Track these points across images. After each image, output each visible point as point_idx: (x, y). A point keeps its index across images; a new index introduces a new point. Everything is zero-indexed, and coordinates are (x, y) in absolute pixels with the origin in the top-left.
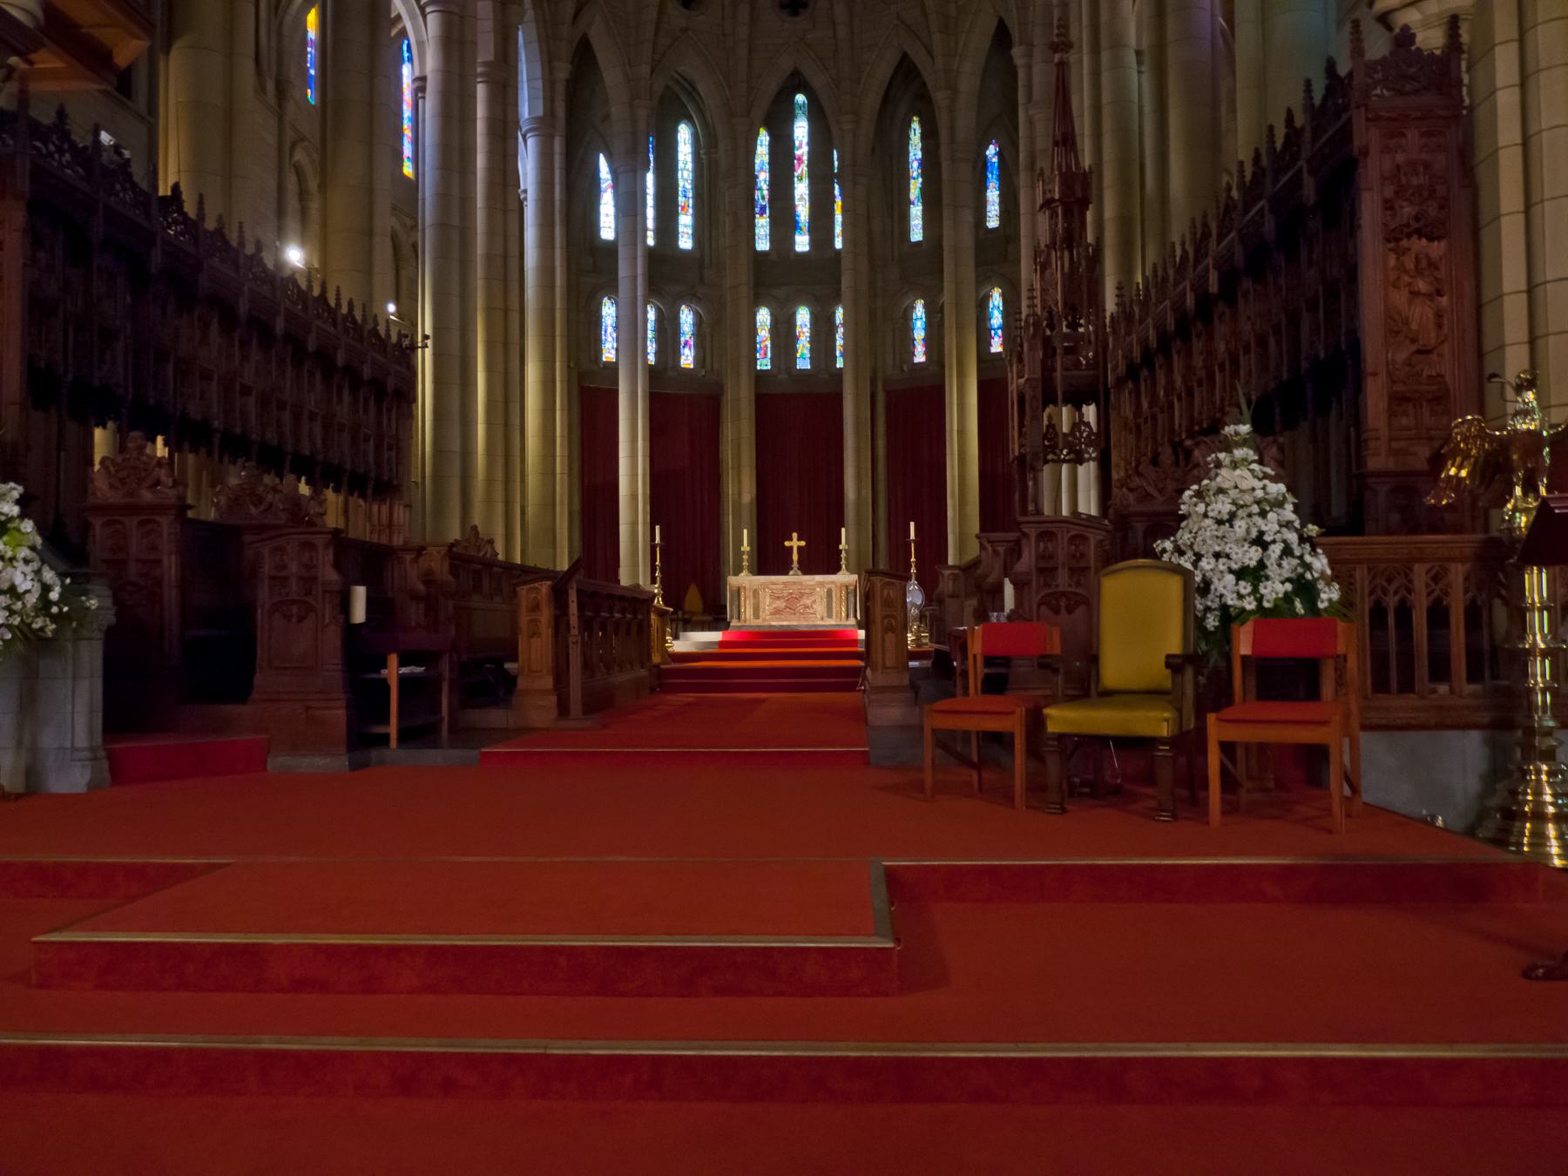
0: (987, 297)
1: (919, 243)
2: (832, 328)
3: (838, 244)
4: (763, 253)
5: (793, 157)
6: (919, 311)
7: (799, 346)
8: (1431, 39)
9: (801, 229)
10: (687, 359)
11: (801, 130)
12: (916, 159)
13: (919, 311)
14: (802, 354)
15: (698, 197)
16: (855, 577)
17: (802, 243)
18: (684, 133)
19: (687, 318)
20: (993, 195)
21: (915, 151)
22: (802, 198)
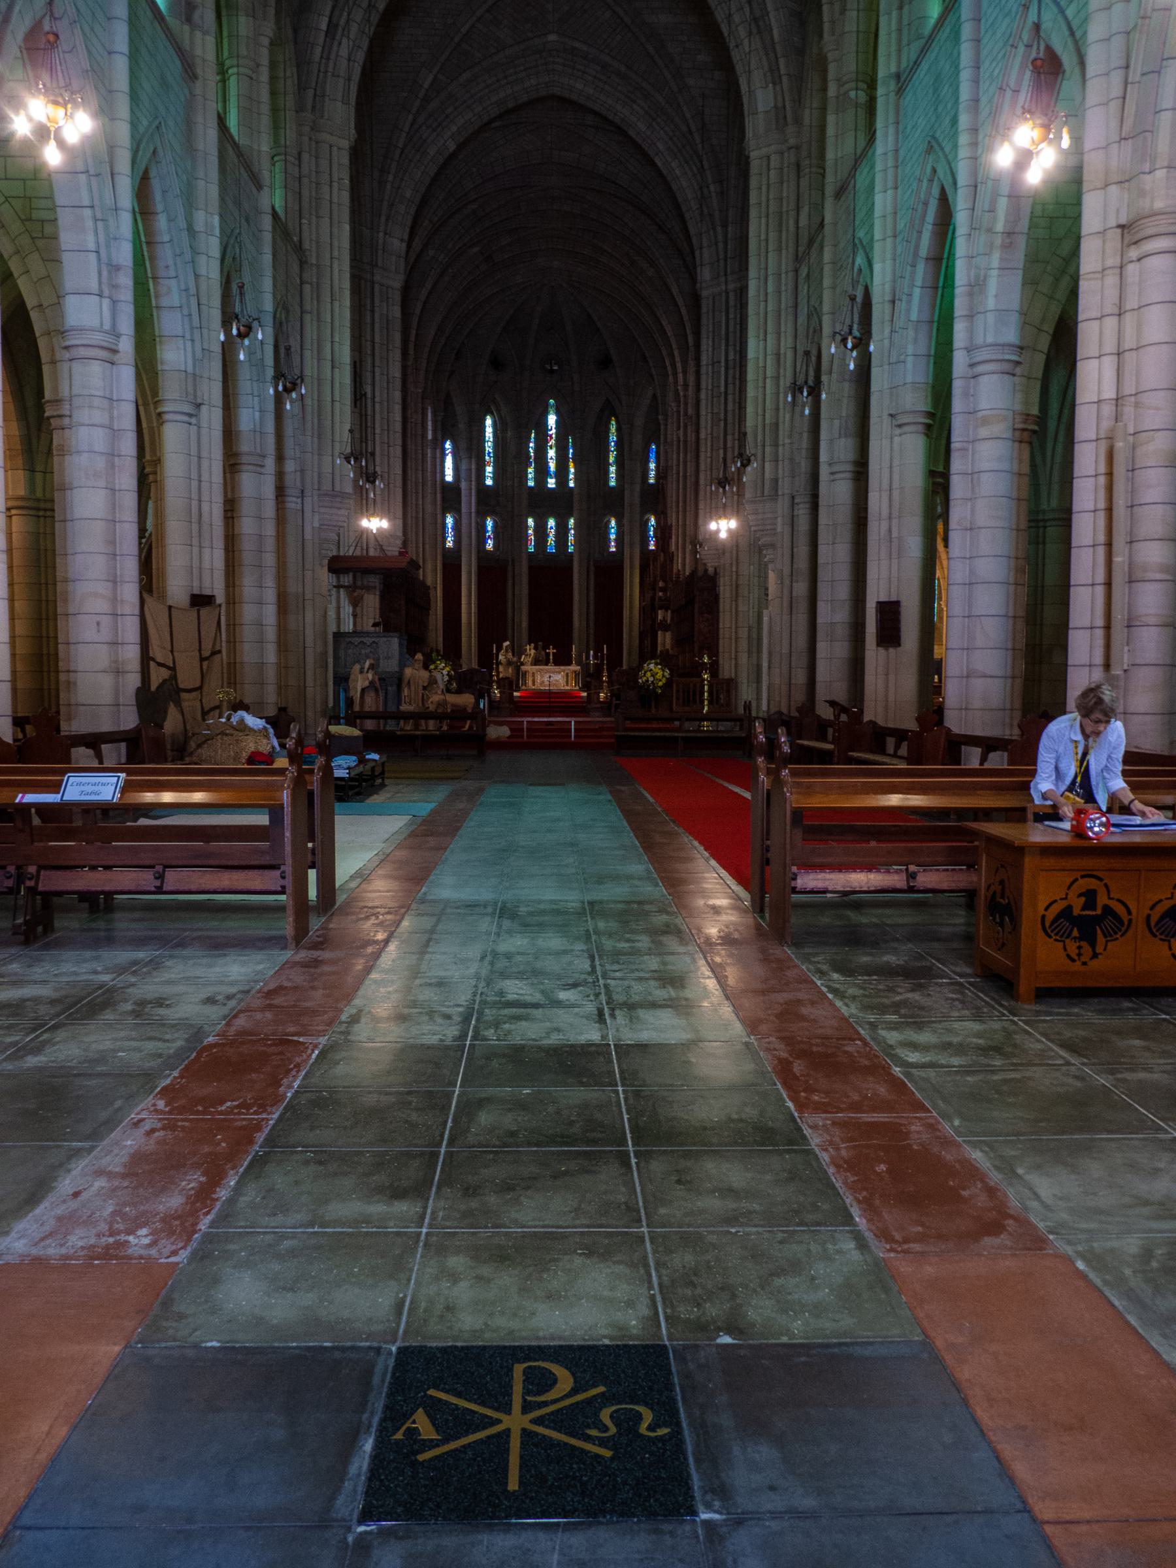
1: (613, 488)
2: (567, 530)
3: (572, 484)
4: (531, 488)
5: (547, 435)
6: (613, 523)
8: (711, 571)
10: (490, 546)
11: (552, 420)
13: (613, 523)
15: (496, 456)
17: (551, 483)
18: (489, 421)
19: (489, 524)
20: (652, 466)
21: (613, 438)
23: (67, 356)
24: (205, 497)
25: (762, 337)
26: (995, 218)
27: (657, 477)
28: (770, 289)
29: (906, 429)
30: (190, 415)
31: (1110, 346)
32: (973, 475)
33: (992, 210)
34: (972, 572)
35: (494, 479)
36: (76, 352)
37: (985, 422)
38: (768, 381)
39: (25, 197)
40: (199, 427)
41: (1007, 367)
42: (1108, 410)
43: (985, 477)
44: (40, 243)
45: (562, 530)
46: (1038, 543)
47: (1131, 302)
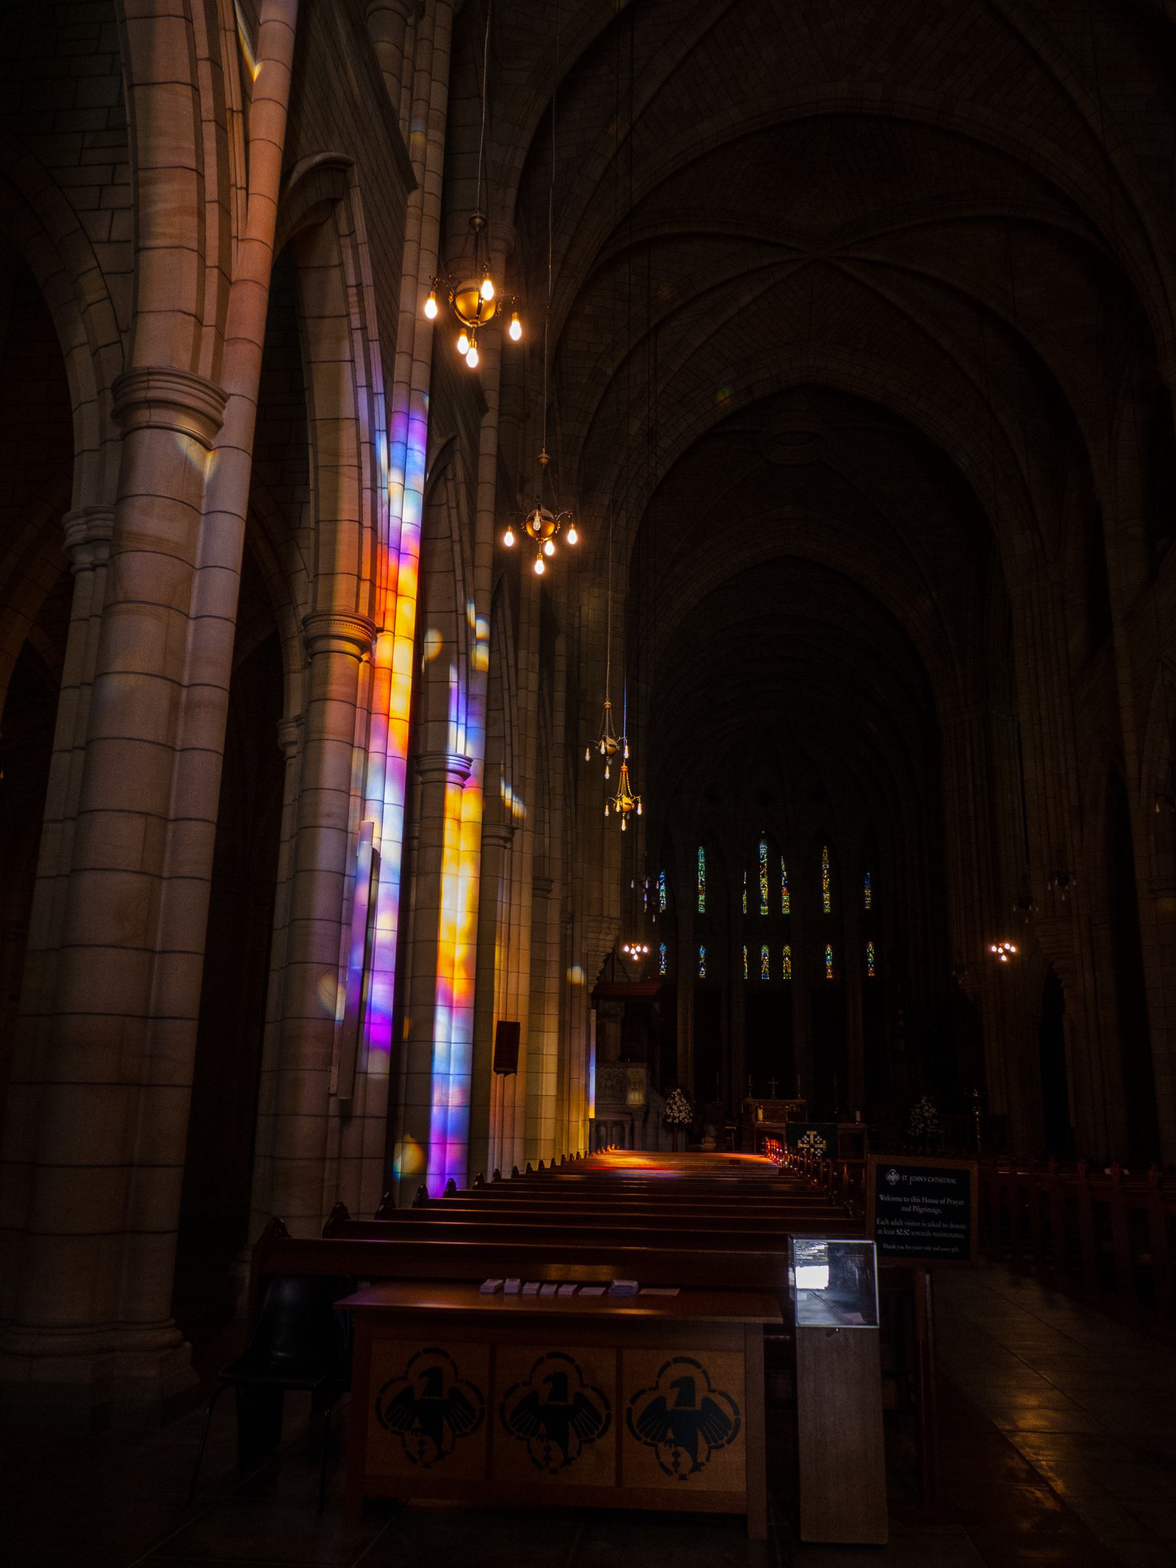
0: (867, 946)
1: (827, 914)
3: (786, 911)
5: (760, 864)
6: (829, 950)
7: (763, 966)
9: (764, 902)
10: (703, 972)
11: (763, 849)
12: (826, 869)
13: (829, 950)
14: (765, 971)
16: (805, 1101)
17: (764, 909)
18: (701, 852)
19: (702, 952)
20: (868, 892)
21: (826, 866)
22: (764, 886)
23: (421, 779)
24: (514, 921)
27: (871, 904)
30: (506, 840)
35: (705, 906)
40: (512, 851)
45: (776, 958)
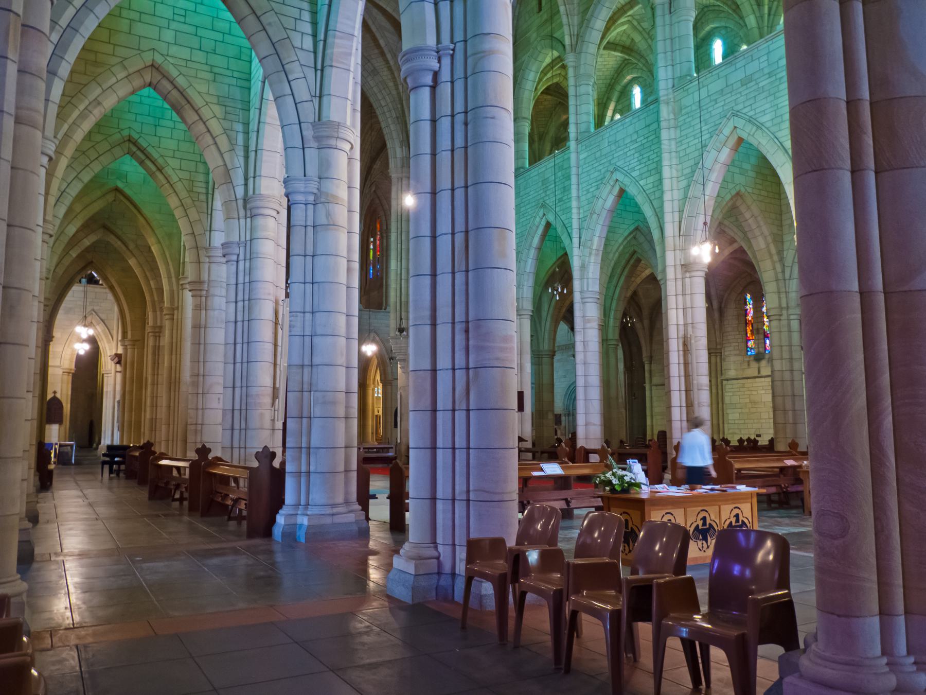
25: (399, 259)
26: (592, 244)
28: (404, 238)
29: (523, 317)
31: (680, 305)
32: (585, 342)
33: (591, 240)
34: (586, 381)
36: (213, 259)
37: (589, 321)
38: (403, 281)
39: (190, 180)
41: (596, 300)
42: (681, 328)
43: (590, 343)
44: (196, 203)
46: (539, 365)
47: (688, 292)
